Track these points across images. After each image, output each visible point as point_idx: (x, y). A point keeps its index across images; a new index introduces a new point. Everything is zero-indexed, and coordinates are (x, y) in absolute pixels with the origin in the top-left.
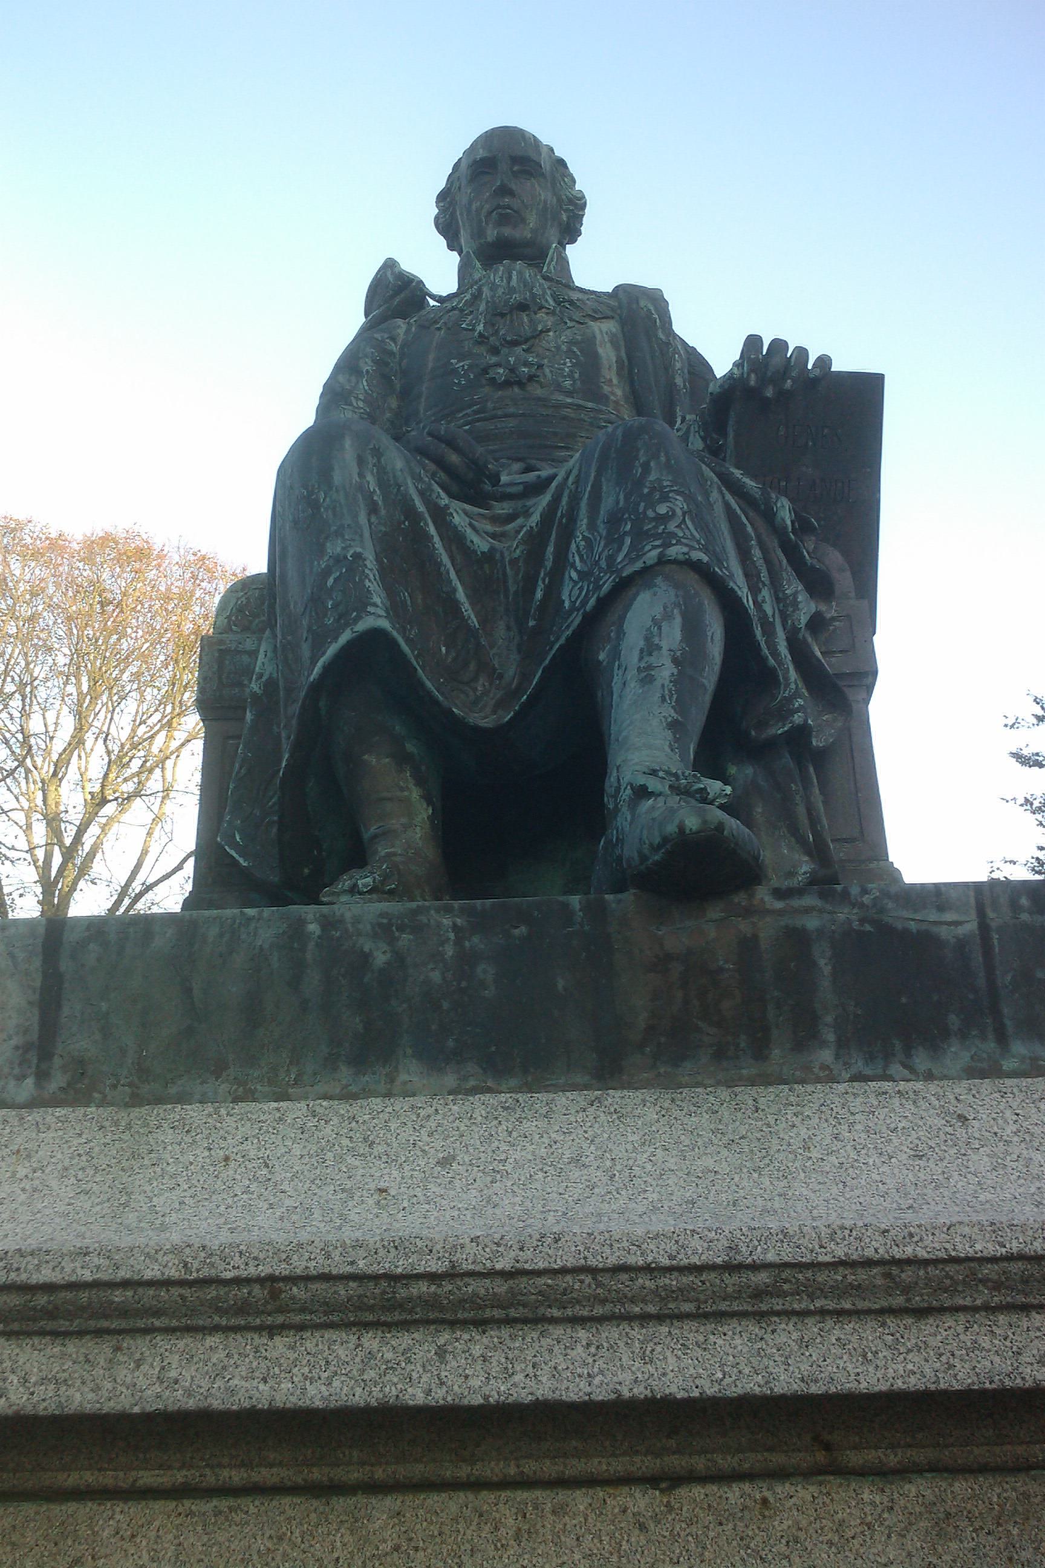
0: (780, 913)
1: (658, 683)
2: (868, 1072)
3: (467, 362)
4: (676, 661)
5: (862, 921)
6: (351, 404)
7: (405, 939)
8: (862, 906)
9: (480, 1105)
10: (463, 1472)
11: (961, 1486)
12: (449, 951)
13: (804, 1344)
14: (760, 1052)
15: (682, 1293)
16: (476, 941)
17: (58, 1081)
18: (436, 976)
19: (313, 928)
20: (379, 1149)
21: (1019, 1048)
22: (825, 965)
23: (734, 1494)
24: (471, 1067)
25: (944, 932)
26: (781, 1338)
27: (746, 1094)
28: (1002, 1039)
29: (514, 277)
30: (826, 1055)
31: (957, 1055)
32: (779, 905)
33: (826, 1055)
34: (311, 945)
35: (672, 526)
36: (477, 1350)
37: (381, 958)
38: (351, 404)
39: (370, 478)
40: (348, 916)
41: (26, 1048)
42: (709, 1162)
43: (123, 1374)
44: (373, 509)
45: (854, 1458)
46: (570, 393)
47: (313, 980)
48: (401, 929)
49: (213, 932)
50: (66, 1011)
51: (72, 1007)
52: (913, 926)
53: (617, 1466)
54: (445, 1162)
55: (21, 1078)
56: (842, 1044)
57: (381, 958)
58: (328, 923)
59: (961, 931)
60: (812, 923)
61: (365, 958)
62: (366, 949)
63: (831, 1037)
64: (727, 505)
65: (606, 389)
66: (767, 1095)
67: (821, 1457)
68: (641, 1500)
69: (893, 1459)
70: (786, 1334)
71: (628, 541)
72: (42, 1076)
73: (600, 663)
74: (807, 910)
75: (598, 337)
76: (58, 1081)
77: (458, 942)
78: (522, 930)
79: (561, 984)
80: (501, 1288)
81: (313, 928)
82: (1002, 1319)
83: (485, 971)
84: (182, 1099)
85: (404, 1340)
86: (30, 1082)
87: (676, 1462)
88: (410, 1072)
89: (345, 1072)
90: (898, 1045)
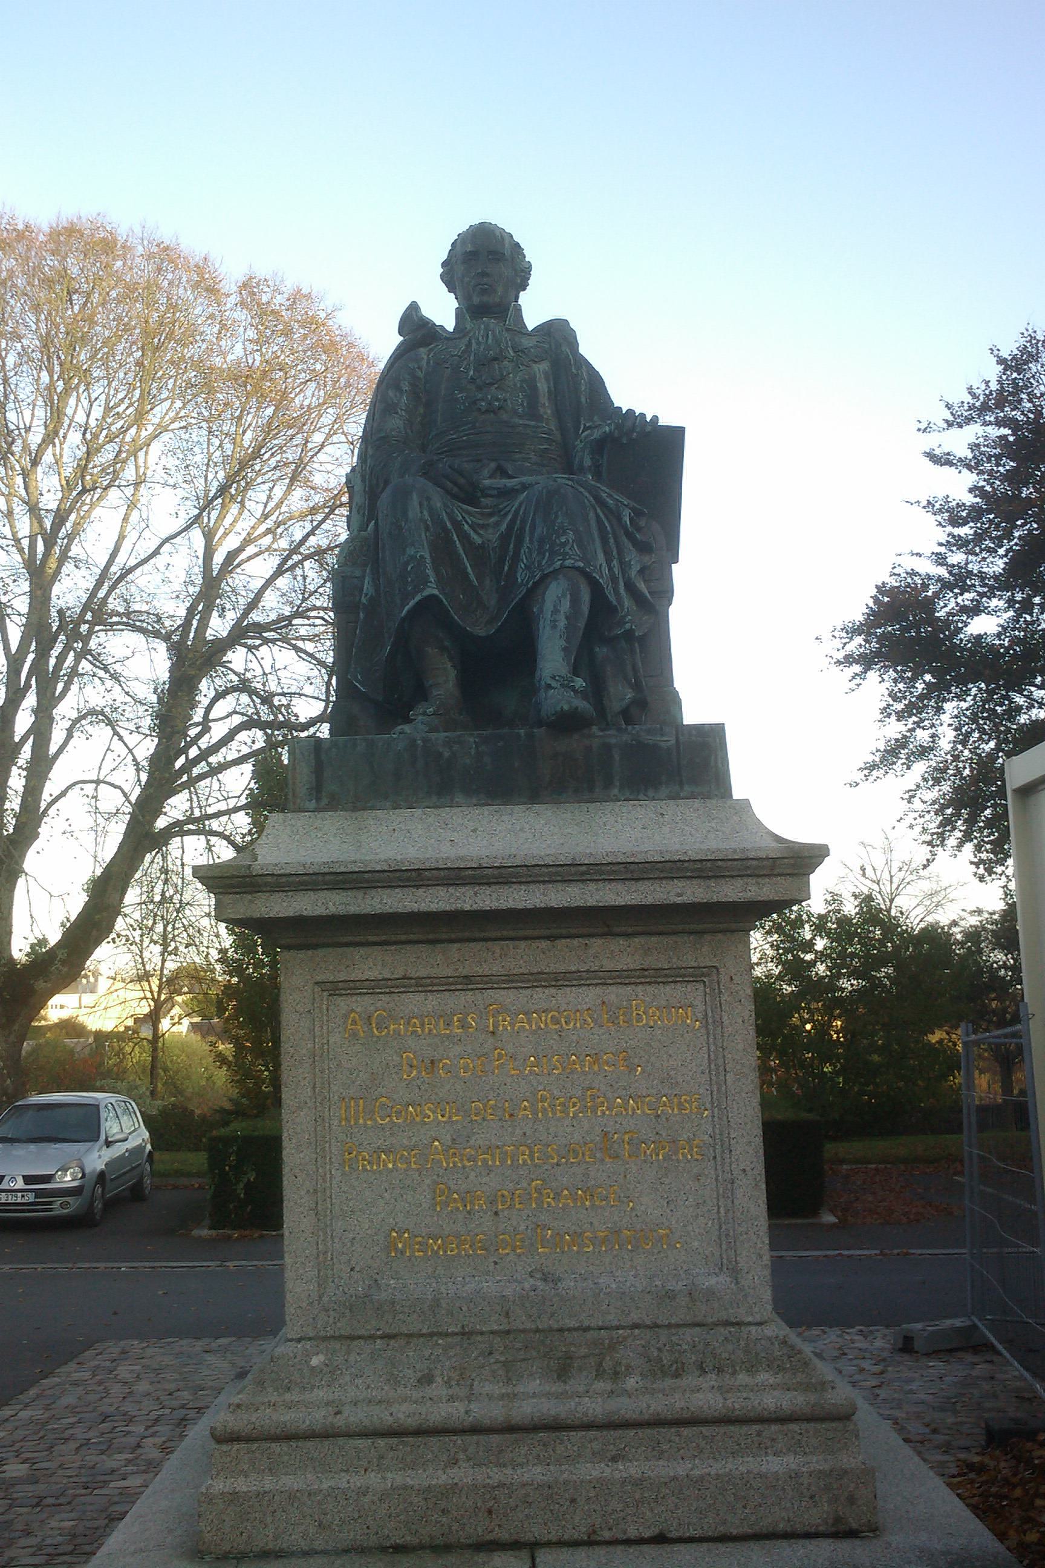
0: (601, 736)
1: (559, 629)
2: (631, 797)
3: (465, 394)
4: (567, 618)
6: (397, 413)
7: (456, 747)
9: (486, 810)
10: (482, 935)
11: (654, 939)
12: (473, 751)
13: (598, 890)
14: (591, 789)
15: (557, 874)
16: (483, 748)
17: (325, 801)
18: (468, 761)
20: (450, 826)
21: (687, 788)
22: (617, 757)
23: (576, 942)
25: (662, 744)
26: (590, 888)
27: (584, 806)
28: (681, 784)
29: (490, 337)
30: (616, 791)
31: (664, 791)
32: (601, 734)
33: (616, 791)
34: (419, 749)
35: (567, 549)
36: (488, 892)
37: (447, 754)
38: (397, 413)
39: (426, 513)
40: (433, 738)
42: (569, 830)
43: (368, 902)
44: (427, 529)
45: (616, 930)
46: (520, 417)
53: (536, 933)
54: (474, 831)
55: (310, 801)
57: (447, 754)
59: (669, 744)
60: (613, 741)
61: (441, 754)
62: (441, 750)
63: (618, 784)
64: (599, 522)
65: (542, 410)
66: (592, 806)
67: (606, 929)
68: (544, 944)
69: (630, 930)
70: (592, 886)
71: (547, 554)
72: (318, 800)
73: (534, 613)
75: (538, 376)
76: (325, 801)
78: (500, 744)
79: (516, 764)
80: (496, 872)
82: (664, 882)
84: (372, 808)
85: (463, 889)
88: (459, 798)
89: (434, 798)
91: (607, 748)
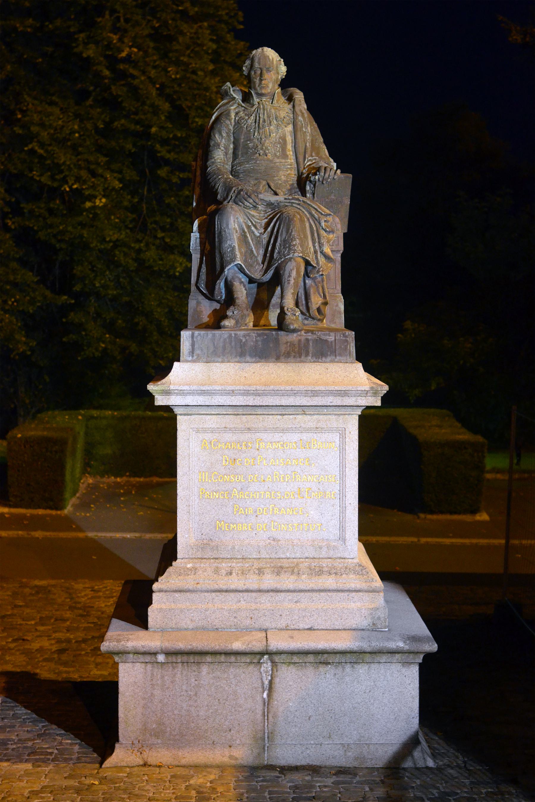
1: (290, 284)
3: (252, 144)
4: (294, 279)
5: (317, 338)
6: (220, 149)
7: (247, 338)
8: (317, 335)
9: (259, 365)
10: (255, 413)
11: (321, 416)
12: (254, 340)
13: (300, 399)
14: (300, 357)
15: (285, 393)
17: (195, 357)
18: (252, 344)
19: (233, 335)
20: (244, 370)
21: (338, 358)
22: (311, 344)
23: (291, 417)
24: (257, 358)
25: (329, 340)
26: (297, 399)
27: (297, 364)
28: (336, 356)
29: (265, 114)
30: (310, 358)
31: (329, 359)
32: (305, 335)
33: (310, 358)
35: (296, 248)
36: (259, 399)
37: (244, 340)
38: (220, 149)
39: (236, 225)
41: (190, 352)
42: (291, 374)
43: (213, 400)
44: (237, 232)
45: (307, 413)
46: (278, 158)
47: (233, 344)
48: (247, 336)
49: (218, 335)
50: (195, 346)
51: (196, 346)
52: (325, 339)
53: (276, 413)
54: (254, 373)
55: (189, 356)
56: (312, 356)
57: (244, 340)
58: (235, 335)
59: (332, 340)
60: (310, 338)
61: (241, 340)
63: (311, 355)
64: (311, 226)
65: (288, 153)
66: (300, 364)
67: (303, 412)
68: (279, 417)
69: (312, 413)
70: (298, 398)
71: (287, 249)
72: (193, 356)
73: (280, 274)
74: (309, 336)
75: (287, 133)
77: (256, 338)
78: (265, 337)
79: (271, 345)
80: (262, 392)
81: (233, 335)
82: (326, 397)
83: (260, 343)
84: (214, 362)
85: (249, 397)
86: (191, 357)
87: (284, 413)
88: (248, 358)
89: (238, 359)
90: (320, 357)
91: (307, 340)
